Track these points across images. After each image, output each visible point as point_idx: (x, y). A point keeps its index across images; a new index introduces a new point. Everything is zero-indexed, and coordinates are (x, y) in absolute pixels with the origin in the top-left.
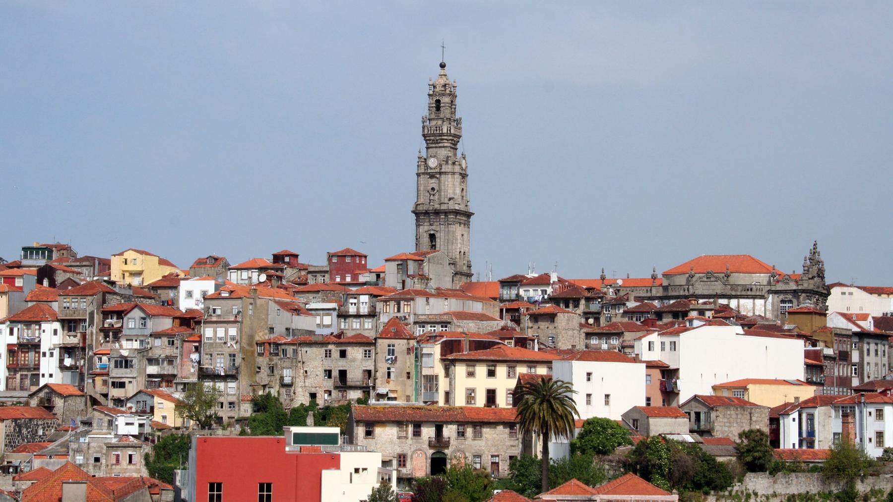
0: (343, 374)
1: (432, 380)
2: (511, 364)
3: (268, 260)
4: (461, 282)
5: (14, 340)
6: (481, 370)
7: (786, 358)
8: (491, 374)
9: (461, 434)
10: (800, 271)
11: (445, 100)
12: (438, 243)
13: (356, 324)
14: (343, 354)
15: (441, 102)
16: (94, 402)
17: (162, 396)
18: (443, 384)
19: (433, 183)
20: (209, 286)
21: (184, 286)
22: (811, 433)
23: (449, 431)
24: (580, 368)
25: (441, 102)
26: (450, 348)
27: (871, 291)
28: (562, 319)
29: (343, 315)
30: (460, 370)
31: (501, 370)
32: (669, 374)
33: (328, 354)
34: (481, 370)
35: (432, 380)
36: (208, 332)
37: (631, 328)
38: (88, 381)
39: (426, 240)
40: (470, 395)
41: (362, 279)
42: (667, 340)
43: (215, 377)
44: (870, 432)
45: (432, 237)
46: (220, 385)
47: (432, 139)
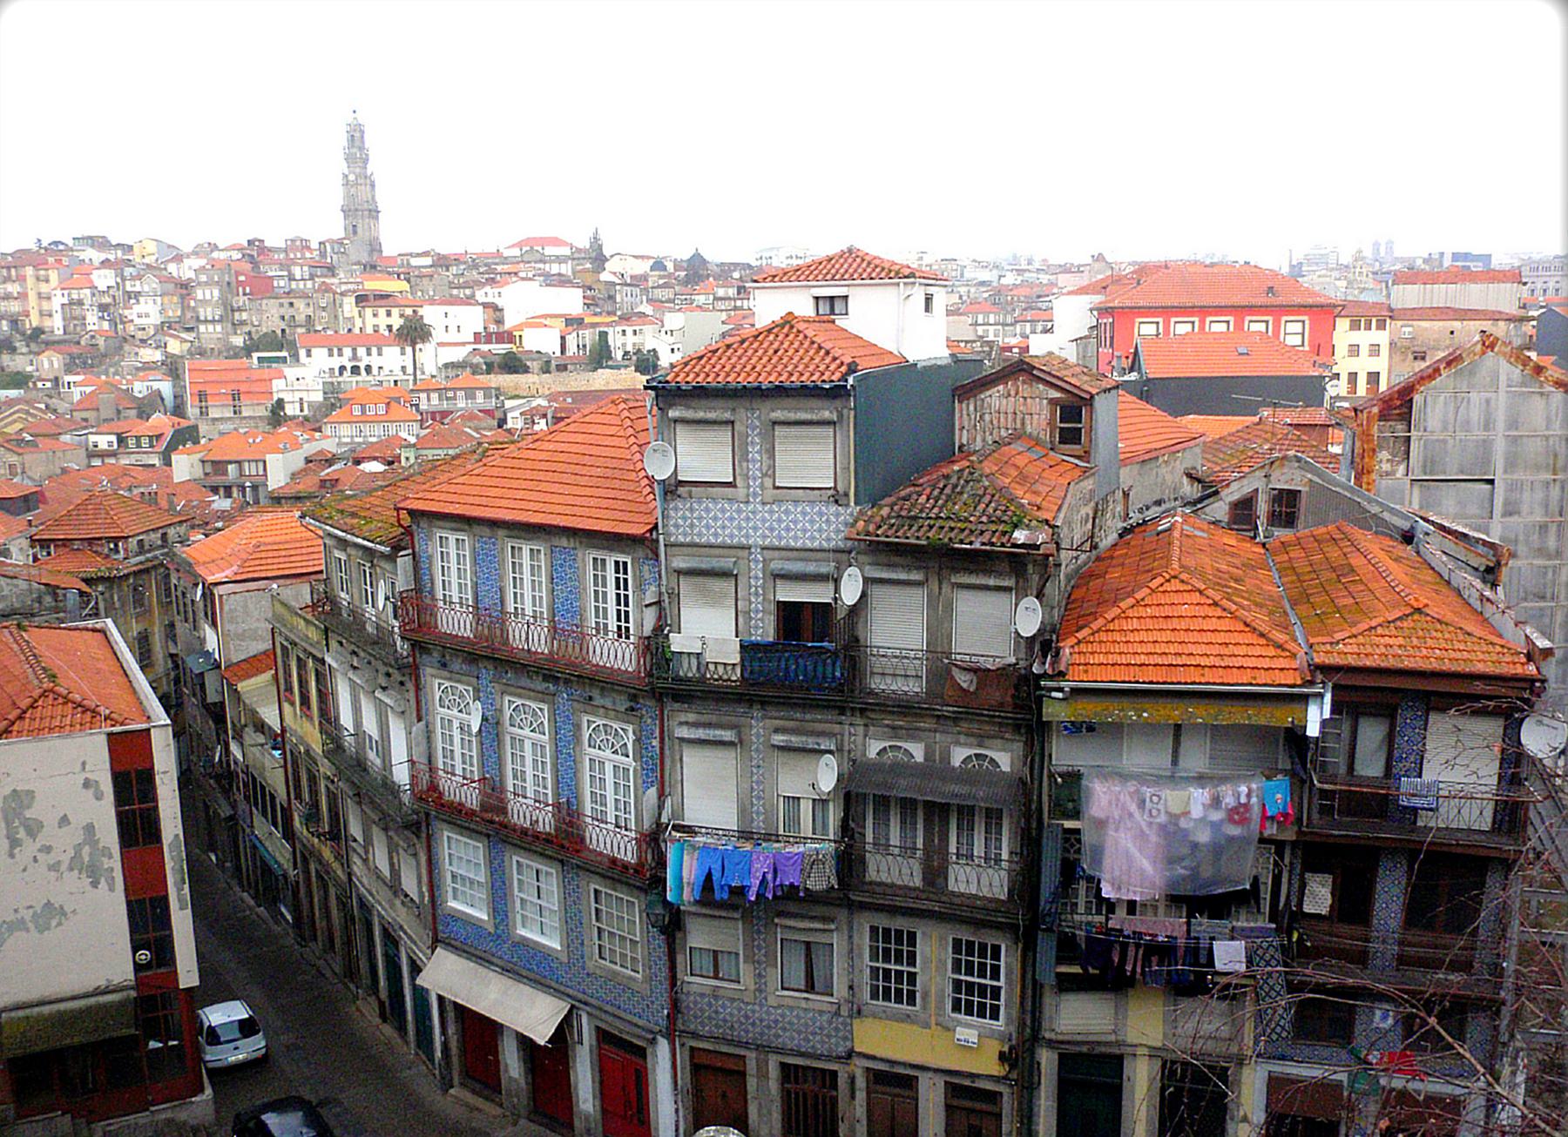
6: (382, 312)
7: (571, 301)
8: (389, 314)
9: (369, 354)
11: (357, 135)
12: (359, 230)
13: (301, 284)
14: (291, 304)
15: (356, 138)
17: (172, 336)
20: (203, 262)
23: (361, 351)
25: (356, 138)
26: (361, 300)
30: (369, 311)
31: (395, 312)
33: (281, 305)
34: (382, 312)
35: (351, 319)
36: (199, 294)
38: (120, 327)
42: (496, 291)
43: (206, 321)
46: (210, 327)
47: (349, 159)
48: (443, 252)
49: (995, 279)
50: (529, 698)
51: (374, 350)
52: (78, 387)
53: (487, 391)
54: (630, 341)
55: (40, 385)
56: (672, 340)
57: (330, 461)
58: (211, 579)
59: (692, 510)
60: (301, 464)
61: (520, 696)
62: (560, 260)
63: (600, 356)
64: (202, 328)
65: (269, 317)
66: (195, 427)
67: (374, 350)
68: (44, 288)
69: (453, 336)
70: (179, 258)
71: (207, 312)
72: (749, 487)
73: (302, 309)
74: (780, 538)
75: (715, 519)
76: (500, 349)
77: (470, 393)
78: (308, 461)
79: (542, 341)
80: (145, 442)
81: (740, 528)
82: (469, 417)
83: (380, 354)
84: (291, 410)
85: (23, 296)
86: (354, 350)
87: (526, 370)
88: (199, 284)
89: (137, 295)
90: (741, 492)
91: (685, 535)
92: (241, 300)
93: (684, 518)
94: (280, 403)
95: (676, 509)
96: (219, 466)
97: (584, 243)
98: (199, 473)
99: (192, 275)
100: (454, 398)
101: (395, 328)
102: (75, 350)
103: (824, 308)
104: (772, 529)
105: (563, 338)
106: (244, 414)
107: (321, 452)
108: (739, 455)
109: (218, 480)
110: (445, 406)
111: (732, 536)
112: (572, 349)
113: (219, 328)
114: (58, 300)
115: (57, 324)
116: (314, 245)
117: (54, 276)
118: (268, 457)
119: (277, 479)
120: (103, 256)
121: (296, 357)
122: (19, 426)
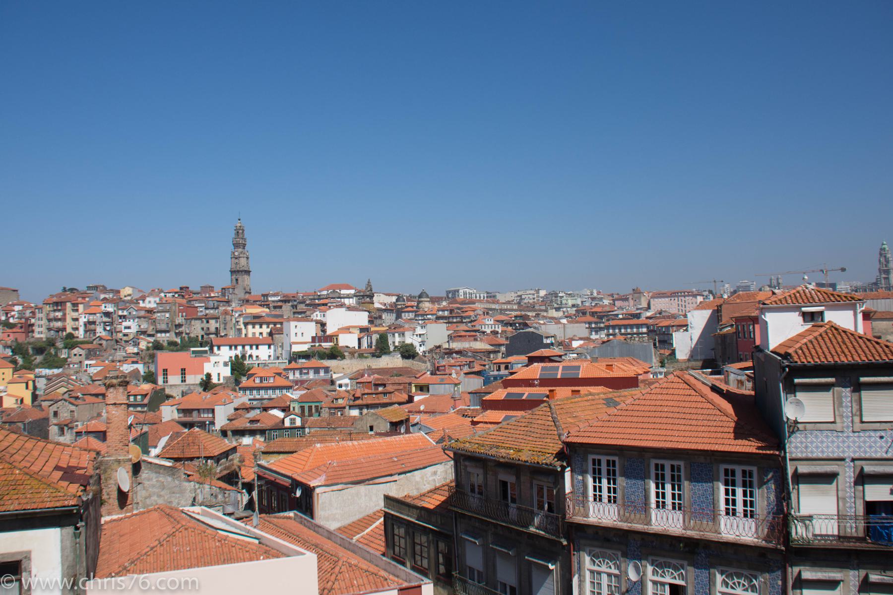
0: (208, 328)
1: (240, 330)
2: (268, 324)
3: (178, 290)
4: (247, 296)
5: (86, 320)
6: (257, 327)
7: (362, 318)
8: (261, 327)
9: (251, 348)
10: (364, 289)
12: (239, 282)
13: (212, 311)
14: (208, 322)
16: (117, 341)
18: (244, 331)
19: (237, 261)
21: (148, 299)
22: (371, 343)
23: (247, 348)
24: (293, 324)
27: (387, 295)
28: (284, 307)
29: (206, 308)
30: (250, 327)
31: (264, 326)
32: (323, 325)
34: (257, 327)
37: (309, 310)
39: (234, 281)
40: (254, 334)
41: (212, 295)
44: (390, 342)
45: (237, 280)
46: (163, 335)
47: (236, 245)
48: (286, 292)
49: (580, 303)
50: (672, 558)
51: (254, 347)
52: (93, 368)
53: (327, 370)
54: (398, 339)
55: (71, 366)
56: (420, 340)
57: (248, 409)
58: (312, 485)
59: (806, 437)
60: (233, 411)
61: (664, 556)
62: (348, 297)
63: (382, 348)
64: (159, 335)
65: (196, 329)
66: (163, 389)
67: (254, 347)
68: (75, 315)
69: (299, 339)
70: (143, 299)
71: (163, 327)
72: (843, 422)
73: (213, 325)
74: (865, 452)
75: (822, 442)
76: (327, 345)
77: (317, 370)
78: (236, 409)
79: (349, 341)
80: (139, 397)
81: (838, 447)
82: (315, 383)
83: (257, 348)
84: (215, 380)
85: (63, 319)
86: (244, 347)
87: (343, 357)
88: (158, 312)
89: (124, 317)
90: (838, 427)
91: (802, 452)
92: (179, 320)
93: (801, 442)
94: (209, 376)
95: (796, 437)
96: (187, 412)
97: (362, 287)
98: (176, 415)
99: (153, 305)
100: (308, 373)
101: (265, 335)
102: (90, 346)
103: (809, 318)
104: (859, 447)
105: (359, 340)
106: (187, 382)
107: (243, 404)
108: (838, 403)
109: (188, 419)
110: (305, 377)
111: (833, 452)
112: (365, 345)
113: (168, 335)
114: (83, 320)
115: (82, 330)
116: (218, 289)
117: (81, 307)
118: (217, 408)
119: (221, 421)
120: (102, 296)
121: (211, 349)
122: (64, 390)
